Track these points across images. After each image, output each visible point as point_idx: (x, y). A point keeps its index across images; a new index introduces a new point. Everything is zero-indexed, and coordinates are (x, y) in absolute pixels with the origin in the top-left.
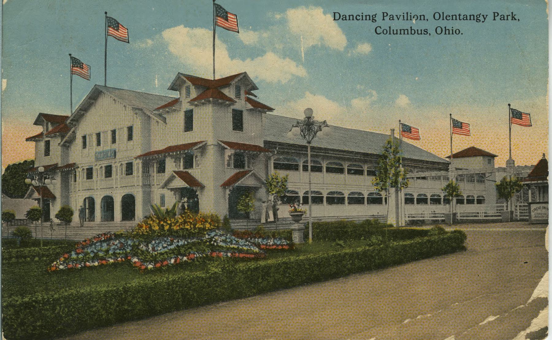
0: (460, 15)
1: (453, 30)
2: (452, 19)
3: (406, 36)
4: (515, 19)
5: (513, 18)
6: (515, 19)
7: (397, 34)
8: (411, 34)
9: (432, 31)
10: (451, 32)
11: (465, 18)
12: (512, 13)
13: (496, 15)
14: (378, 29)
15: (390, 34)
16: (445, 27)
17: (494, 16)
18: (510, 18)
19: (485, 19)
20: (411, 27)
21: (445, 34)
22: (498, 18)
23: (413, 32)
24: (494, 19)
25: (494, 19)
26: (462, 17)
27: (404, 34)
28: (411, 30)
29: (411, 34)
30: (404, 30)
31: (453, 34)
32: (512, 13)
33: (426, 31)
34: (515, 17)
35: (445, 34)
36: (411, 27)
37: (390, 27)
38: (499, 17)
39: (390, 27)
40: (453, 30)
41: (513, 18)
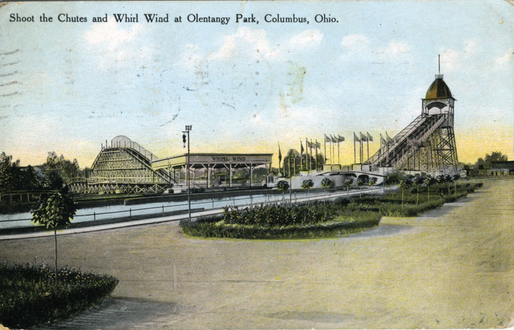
0: (209, 18)
2: (204, 21)
3: (290, 23)
4: (255, 21)
5: (253, 20)
6: (255, 21)
7: (284, 21)
11: (213, 20)
12: (252, 15)
13: (238, 17)
14: (268, 17)
15: (278, 21)
17: (237, 18)
18: (251, 20)
19: (228, 21)
21: (325, 21)
22: (241, 21)
24: (237, 21)
25: (237, 21)
26: (211, 20)
27: (289, 21)
29: (294, 21)
32: (252, 15)
34: (255, 19)
35: (325, 21)
38: (242, 19)
41: (253, 20)
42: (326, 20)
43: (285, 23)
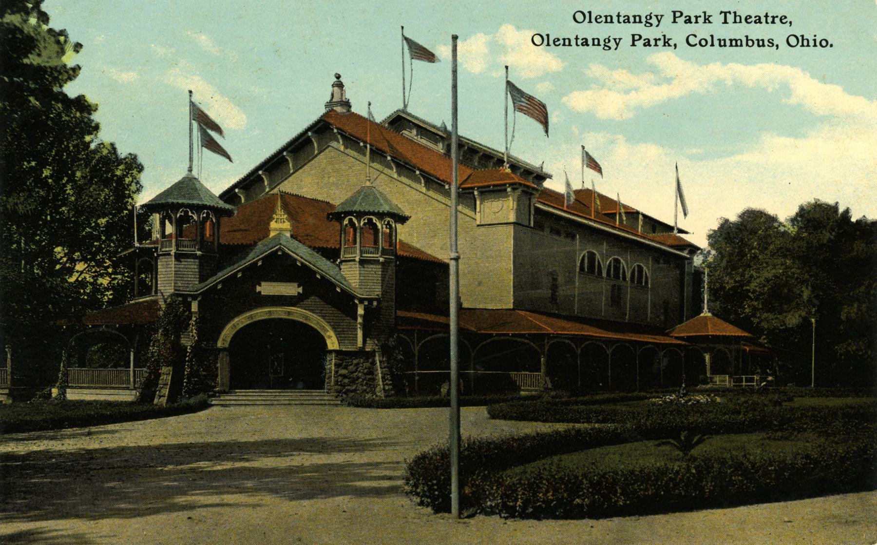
1: (815, 40)
8: (747, 45)
9: (780, 40)
10: (812, 43)
15: (712, 45)
16: (803, 36)
20: (747, 37)
23: (750, 43)
28: (747, 40)
30: (736, 41)
31: (815, 45)
33: (771, 42)
35: (803, 45)
36: (747, 37)
37: (712, 36)
39: (712, 36)
40: (815, 40)
42: (805, 43)
43: (728, 48)
